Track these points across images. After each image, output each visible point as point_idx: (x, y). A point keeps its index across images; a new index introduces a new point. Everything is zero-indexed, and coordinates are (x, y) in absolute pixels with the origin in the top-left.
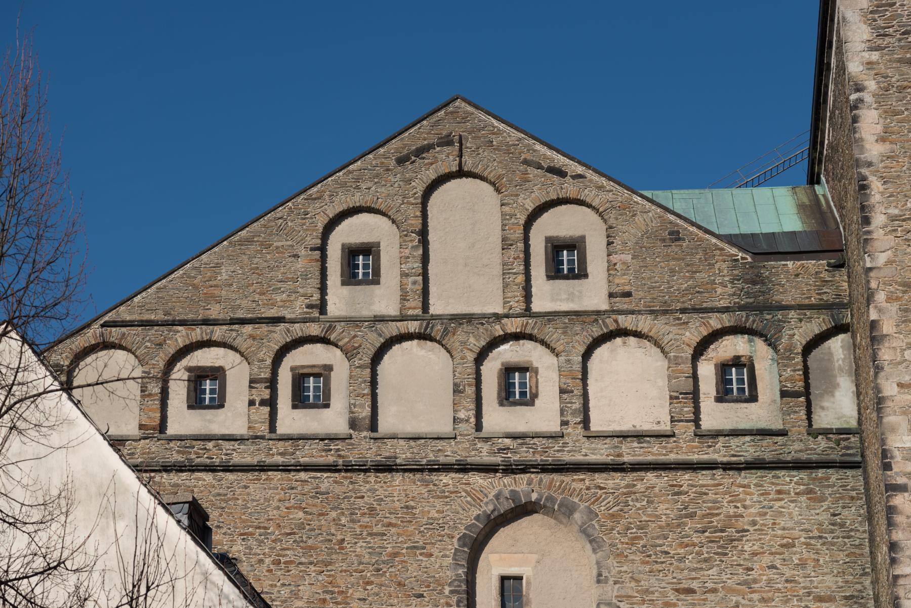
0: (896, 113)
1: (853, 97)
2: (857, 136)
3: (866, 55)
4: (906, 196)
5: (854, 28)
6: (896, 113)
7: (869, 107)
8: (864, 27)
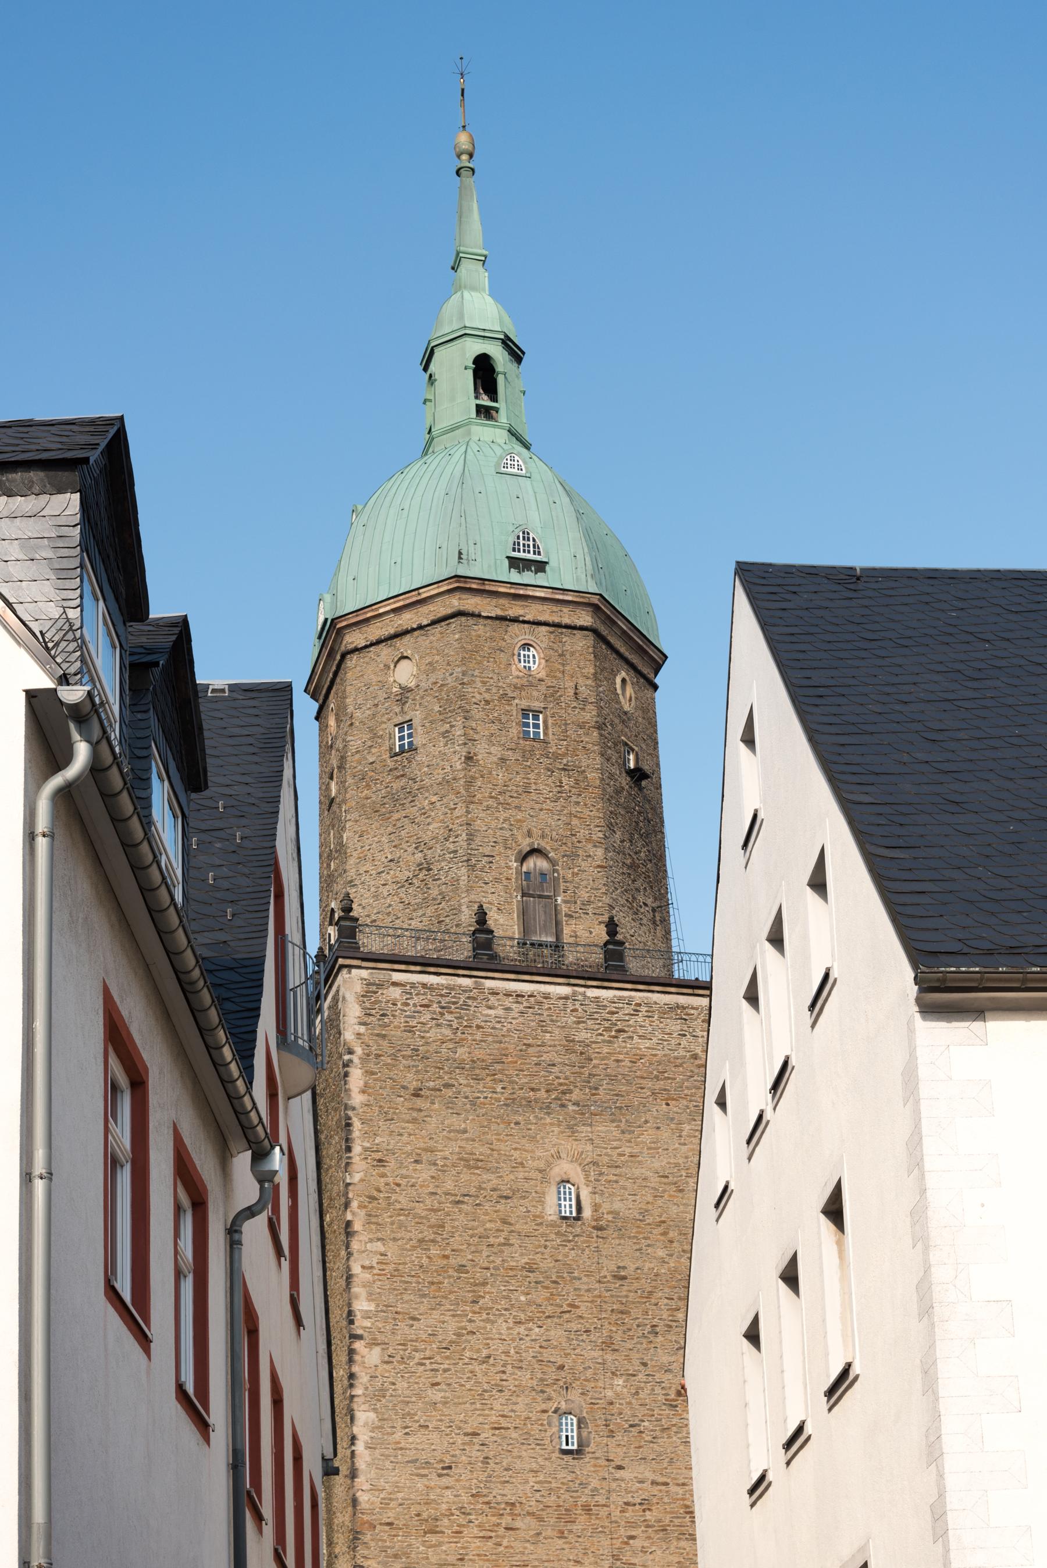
0: (373, 1073)
1: (346, 1057)
2: (347, 1086)
3: (357, 1027)
4: (375, 1134)
5: (350, 1006)
6: (373, 1073)
7: (356, 1067)
8: (357, 1006)
